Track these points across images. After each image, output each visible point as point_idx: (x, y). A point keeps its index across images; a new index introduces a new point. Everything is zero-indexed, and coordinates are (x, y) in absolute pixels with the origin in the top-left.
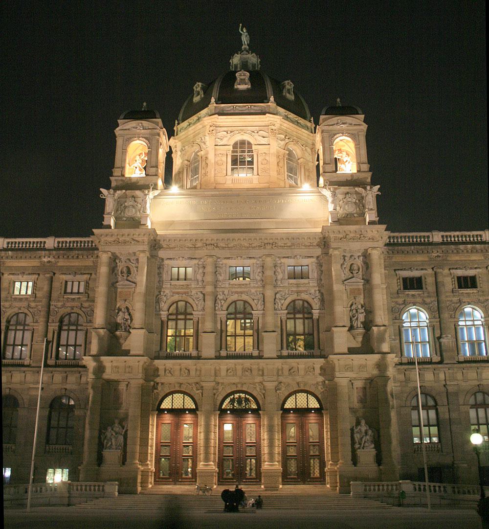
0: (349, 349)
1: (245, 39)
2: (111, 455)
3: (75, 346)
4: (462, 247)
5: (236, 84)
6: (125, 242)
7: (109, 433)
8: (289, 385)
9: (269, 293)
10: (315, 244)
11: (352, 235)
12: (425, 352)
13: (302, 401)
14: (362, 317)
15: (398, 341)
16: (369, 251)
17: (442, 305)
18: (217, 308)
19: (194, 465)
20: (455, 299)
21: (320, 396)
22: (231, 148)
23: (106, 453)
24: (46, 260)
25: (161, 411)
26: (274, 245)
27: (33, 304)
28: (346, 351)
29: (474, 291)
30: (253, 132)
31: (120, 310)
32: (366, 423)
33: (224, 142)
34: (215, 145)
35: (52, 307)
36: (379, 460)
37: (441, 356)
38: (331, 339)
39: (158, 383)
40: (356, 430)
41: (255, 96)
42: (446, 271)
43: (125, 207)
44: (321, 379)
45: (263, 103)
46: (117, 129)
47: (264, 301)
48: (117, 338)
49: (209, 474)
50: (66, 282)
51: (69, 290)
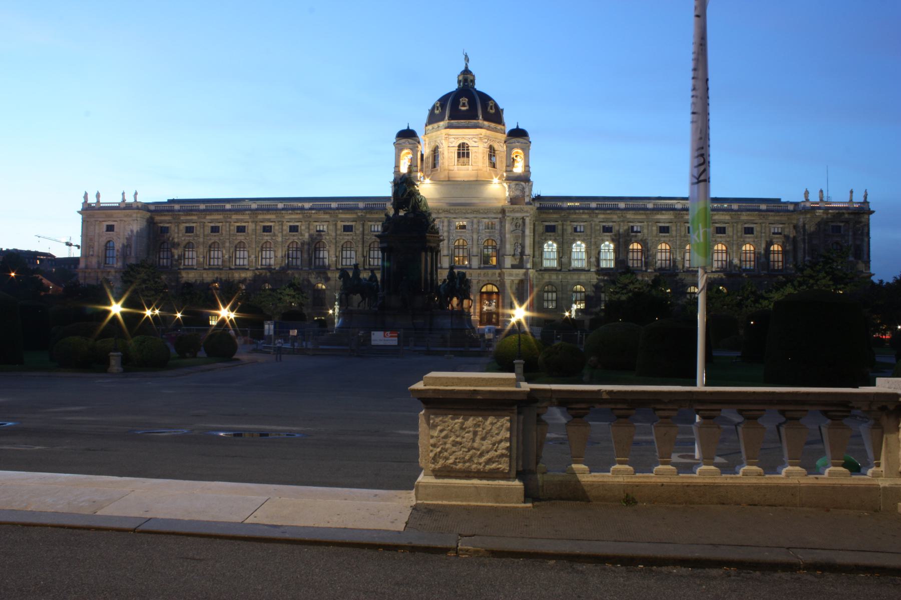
4: (577, 211)
5: (460, 106)
8: (484, 281)
9: (475, 237)
11: (517, 209)
12: (555, 264)
13: (490, 288)
14: (519, 250)
15: (540, 259)
16: (525, 218)
17: (565, 241)
20: (572, 238)
21: (498, 286)
22: (457, 148)
24: (360, 214)
26: (478, 212)
27: (355, 238)
28: (510, 266)
30: (470, 139)
33: (453, 145)
35: (365, 239)
37: (561, 267)
42: (568, 223)
44: (499, 279)
50: (371, 225)
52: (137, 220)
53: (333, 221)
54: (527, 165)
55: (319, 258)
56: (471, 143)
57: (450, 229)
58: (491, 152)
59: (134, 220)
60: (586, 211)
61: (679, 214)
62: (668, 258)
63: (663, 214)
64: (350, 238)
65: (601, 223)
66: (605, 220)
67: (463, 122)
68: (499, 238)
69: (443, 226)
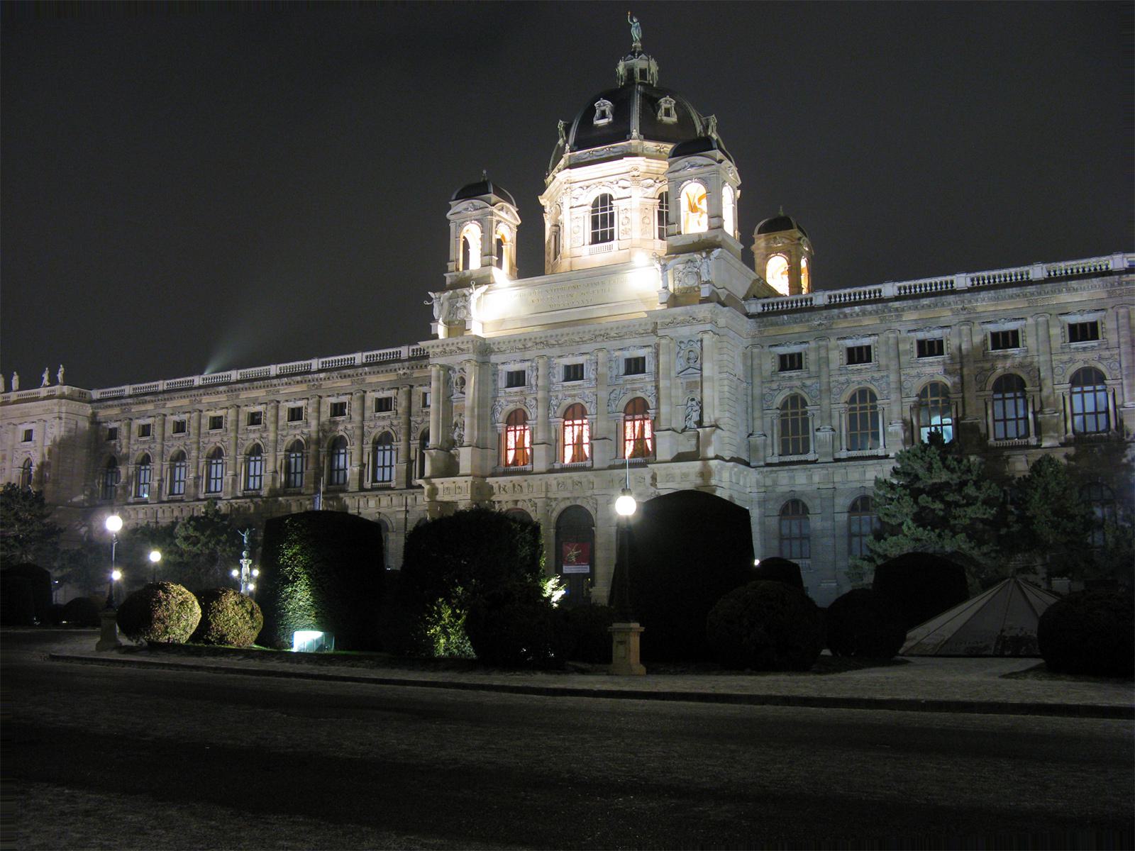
4: (847, 310)
5: (595, 119)
6: (451, 352)
10: (650, 331)
14: (695, 417)
18: (550, 415)
26: (606, 336)
27: (395, 422)
29: (867, 365)
31: (456, 425)
34: (571, 208)
35: (412, 423)
39: (494, 502)
42: (833, 342)
43: (457, 308)
45: (625, 139)
46: (450, 212)
47: (597, 404)
52: (60, 418)
53: (358, 391)
54: (715, 213)
55: (339, 470)
56: (616, 192)
58: (661, 207)
60: (869, 307)
61: (1120, 284)
62: (1101, 408)
63: (1075, 290)
64: (387, 423)
65: (912, 334)
66: (920, 325)
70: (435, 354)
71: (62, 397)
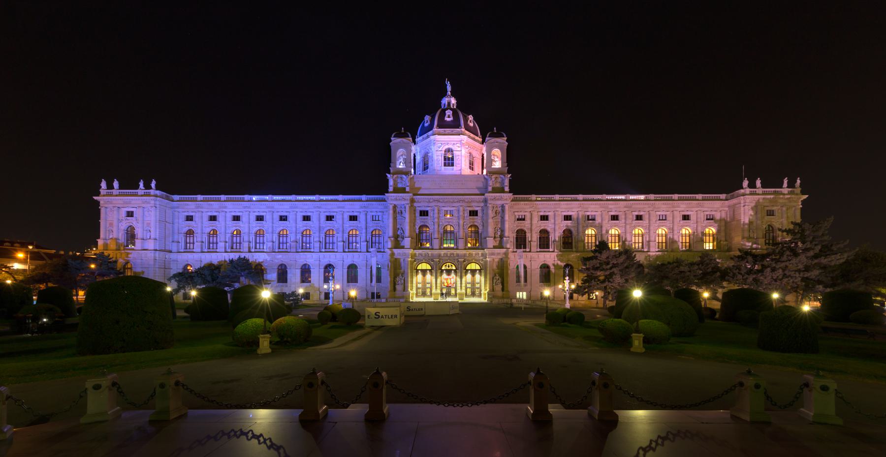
0: (493, 246)
1: (449, 88)
2: (399, 288)
3: (379, 243)
6: (400, 199)
7: (397, 279)
9: (461, 222)
11: (498, 198)
19: (431, 291)
22: (443, 152)
23: (397, 287)
25: (417, 270)
28: (492, 247)
32: (499, 275)
33: (440, 149)
36: (503, 290)
38: (486, 242)
40: (494, 278)
41: (455, 124)
45: (458, 128)
48: (398, 241)
49: (438, 294)
51: (374, 219)
52: (156, 207)
56: (454, 148)
57: (439, 217)
59: (152, 207)
67: (448, 130)
68: (482, 224)
69: (434, 214)
70: (391, 200)
71: (156, 196)
